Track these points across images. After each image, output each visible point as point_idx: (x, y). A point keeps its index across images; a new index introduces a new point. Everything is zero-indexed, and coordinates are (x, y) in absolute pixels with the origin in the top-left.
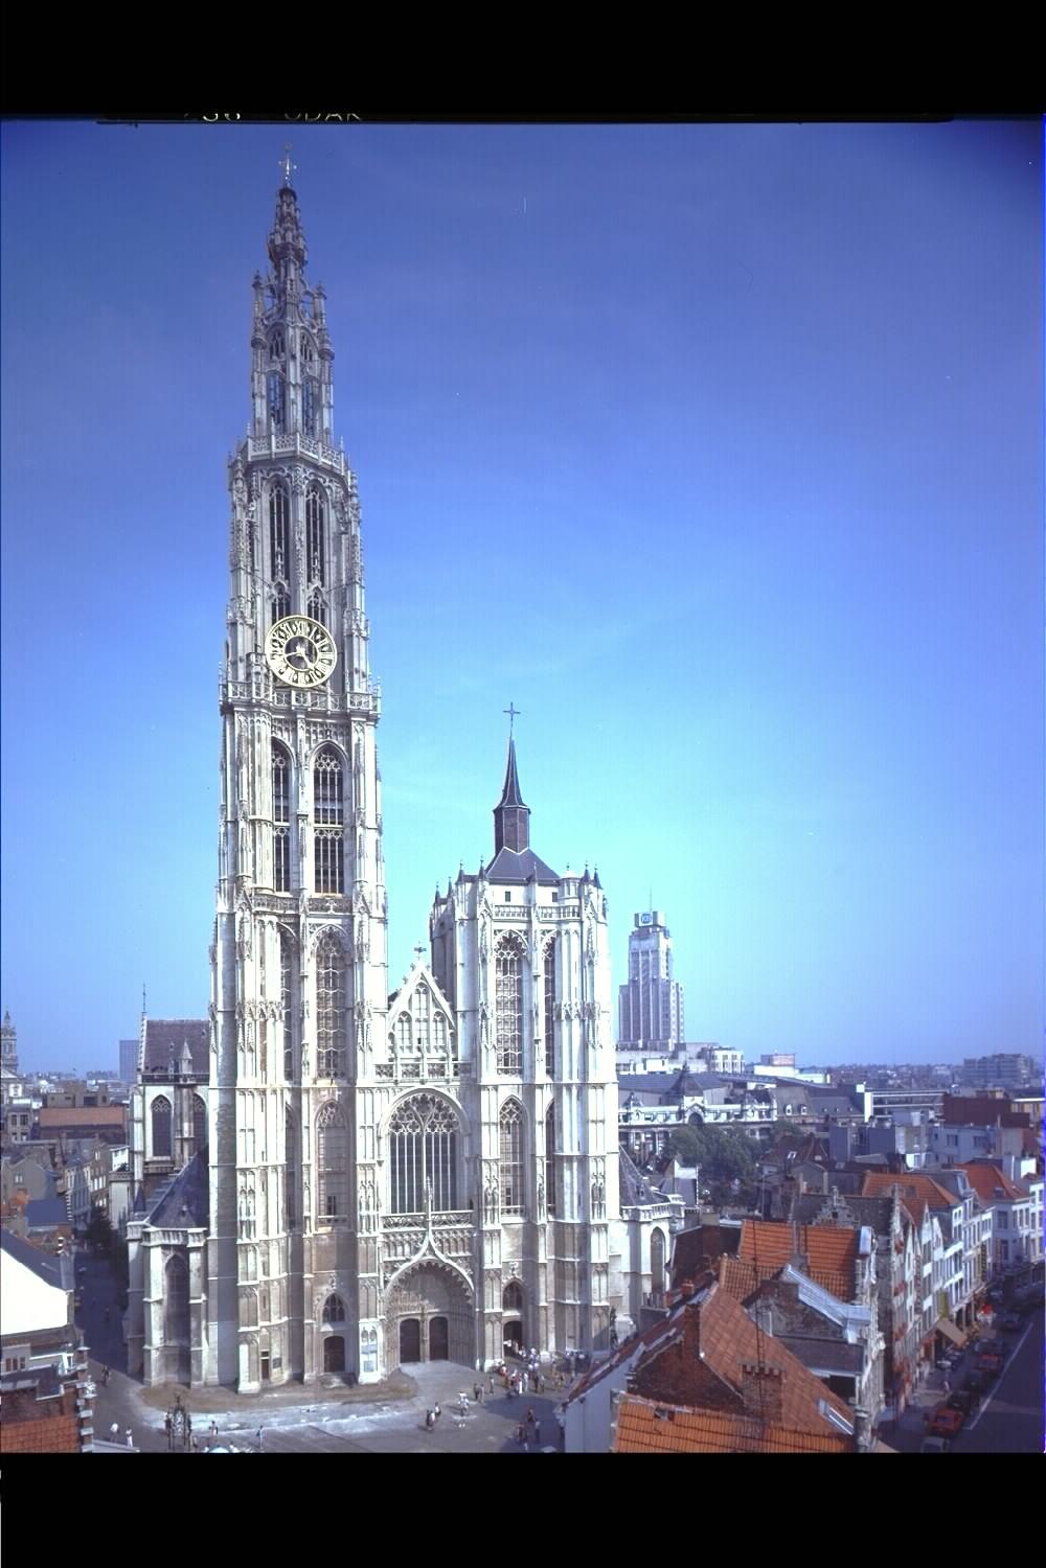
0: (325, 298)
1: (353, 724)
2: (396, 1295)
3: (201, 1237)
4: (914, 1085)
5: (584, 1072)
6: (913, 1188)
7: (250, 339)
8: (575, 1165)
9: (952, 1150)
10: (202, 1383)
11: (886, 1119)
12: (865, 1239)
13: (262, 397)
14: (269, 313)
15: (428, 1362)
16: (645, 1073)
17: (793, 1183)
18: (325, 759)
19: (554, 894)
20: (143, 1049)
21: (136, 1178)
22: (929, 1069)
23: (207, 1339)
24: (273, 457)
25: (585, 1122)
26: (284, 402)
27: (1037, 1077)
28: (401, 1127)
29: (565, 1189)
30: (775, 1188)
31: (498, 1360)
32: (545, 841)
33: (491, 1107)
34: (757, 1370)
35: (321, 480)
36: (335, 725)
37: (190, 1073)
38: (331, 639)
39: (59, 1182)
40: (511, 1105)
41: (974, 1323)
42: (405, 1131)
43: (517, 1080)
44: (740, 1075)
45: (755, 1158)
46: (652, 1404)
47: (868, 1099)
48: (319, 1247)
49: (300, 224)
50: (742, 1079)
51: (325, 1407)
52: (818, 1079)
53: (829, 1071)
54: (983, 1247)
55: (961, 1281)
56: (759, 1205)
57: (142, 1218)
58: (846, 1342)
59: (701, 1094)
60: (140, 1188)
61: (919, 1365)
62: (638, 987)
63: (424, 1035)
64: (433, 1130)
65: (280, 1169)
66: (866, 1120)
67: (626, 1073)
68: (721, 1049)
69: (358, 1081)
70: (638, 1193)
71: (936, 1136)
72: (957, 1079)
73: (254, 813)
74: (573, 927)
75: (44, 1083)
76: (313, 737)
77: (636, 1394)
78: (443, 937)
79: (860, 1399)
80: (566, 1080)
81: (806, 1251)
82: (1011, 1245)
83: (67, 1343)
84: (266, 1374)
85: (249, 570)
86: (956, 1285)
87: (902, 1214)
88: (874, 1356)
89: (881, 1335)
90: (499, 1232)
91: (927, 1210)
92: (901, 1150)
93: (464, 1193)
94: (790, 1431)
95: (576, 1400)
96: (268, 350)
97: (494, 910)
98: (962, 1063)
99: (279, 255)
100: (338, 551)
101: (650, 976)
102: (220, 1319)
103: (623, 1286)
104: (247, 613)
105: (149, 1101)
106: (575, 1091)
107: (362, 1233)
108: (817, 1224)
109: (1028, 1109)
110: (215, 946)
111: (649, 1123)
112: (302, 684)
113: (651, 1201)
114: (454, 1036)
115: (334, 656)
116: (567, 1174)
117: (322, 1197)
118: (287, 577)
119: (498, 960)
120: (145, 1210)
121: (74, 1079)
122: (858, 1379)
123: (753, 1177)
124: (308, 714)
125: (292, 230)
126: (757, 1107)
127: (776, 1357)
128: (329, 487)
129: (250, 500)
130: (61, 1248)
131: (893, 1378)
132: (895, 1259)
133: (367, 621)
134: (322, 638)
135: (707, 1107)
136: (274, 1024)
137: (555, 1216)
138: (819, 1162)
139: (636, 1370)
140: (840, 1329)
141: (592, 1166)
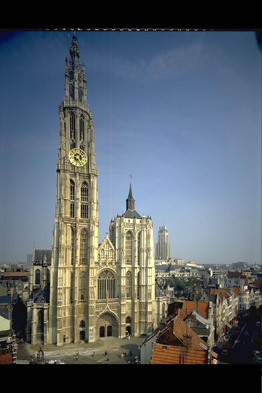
0: (85, 66)
1: (91, 177)
2: (99, 320)
3: (47, 306)
4: (222, 269)
5: (147, 264)
6: (221, 293)
7: (65, 74)
8: (144, 287)
9: (230, 284)
10: (47, 343)
11: (216, 276)
12: (211, 304)
13: (68, 90)
14: (69, 68)
15: (107, 337)
16: (161, 265)
17: (195, 291)
18: (84, 185)
19: (140, 221)
20: (34, 257)
21: (30, 291)
22: (225, 265)
23: (48, 332)
24: (71, 106)
25: (147, 276)
26: (74, 92)
27: (248, 267)
28: (101, 277)
29: (142, 293)
30: (191, 293)
31: (124, 336)
32: (138, 208)
33: (124, 273)
34: (186, 336)
35: (84, 114)
36: (87, 177)
37: (46, 263)
38: (86, 155)
39: (9, 292)
40: (129, 272)
41: (234, 323)
42: (102, 279)
43: (131, 266)
44: (183, 266)
45: (187, 285)
46: (162, 345)
47: (211, 271)
48: (79, 308)
49: (78, 47)
50: (184, 266)
51: (80, 349)
52: (201, 267)
53: (203, 265)
54: (236, 306)
55: (231, 314)
56: (187, 296)
57: (32, 301)
58: (206, 329)
59: (174, 270)
60: (31, 293)
61: (222, 333)
62: (160, 244)
63: (107, 254)
64: (109, 278)
65: (69, 288)
66: (211, 277)
67: (157, 265)
68: (179, 259)
69: (90, 266)
70: (159, 294)
71: (226, 281)
72: (231, 267)
73: (65, 198)
74: (145, 229)
75: (5, 265)
76: (81, 179)
77: (158, 343)
78: (113, 230)
79: (209, 342)
80: (142, 266)
81: (198, 307)
82: (242, 306)
83: (10, 334)
84: (64, 341)
85: (65, 136)
86: (230, 315)
87: (219, 299)
88: (212, 332)
89: (214, 327)
90: (125, 304)
91: (224, 297)
92: (218, 283)
93: (116, 294)
94: (193, 350)
95: (143, 345)
96: (69, 78)
97: (126, 224)
98: (232, 264)
99: (73, 54)
100: (88, 132)
101: (163, 242)
102: (52, 327)
103: (155, 317)
104: (64, 146)
105: (35, 270)
106: (144, 269)
107: (90, 305)
108: (200, 301)
109: (246, 275)
110: (54, 231)
111: (162, 277)
112: (78, 165)
113: (162, 296)
114: (115, 255)
115: (86, 159)
116: (142, 290)
117: (80, 295)
118: (75, 138)
119: (126, 237)
120: (32, 299)
121: (14, 264)
122: (208, 337)
123: (186, 290)
124: (79, 174)
125: (76, 48)
126: (187, 273)
127: (191, 333)
128: (86, 116)
129: (65, 117)
130: (9, 309)
131: (216, 336)
132: (217, 309)
133: (95, 151)
134: (84, 154)
135: (175, 273)
136: (69, 251)
137: (139, 300)
138: (201, 286)
139: (158, 337)
140: (205, 326)
141: (148, 287)
